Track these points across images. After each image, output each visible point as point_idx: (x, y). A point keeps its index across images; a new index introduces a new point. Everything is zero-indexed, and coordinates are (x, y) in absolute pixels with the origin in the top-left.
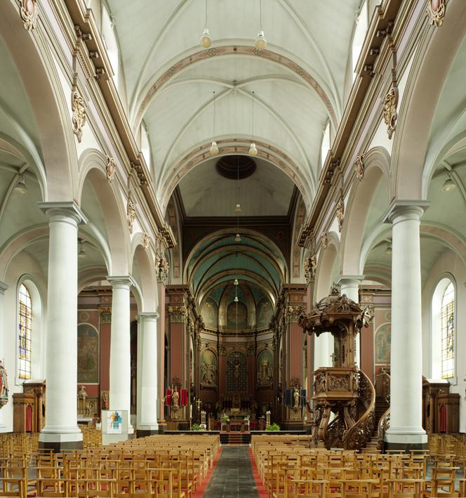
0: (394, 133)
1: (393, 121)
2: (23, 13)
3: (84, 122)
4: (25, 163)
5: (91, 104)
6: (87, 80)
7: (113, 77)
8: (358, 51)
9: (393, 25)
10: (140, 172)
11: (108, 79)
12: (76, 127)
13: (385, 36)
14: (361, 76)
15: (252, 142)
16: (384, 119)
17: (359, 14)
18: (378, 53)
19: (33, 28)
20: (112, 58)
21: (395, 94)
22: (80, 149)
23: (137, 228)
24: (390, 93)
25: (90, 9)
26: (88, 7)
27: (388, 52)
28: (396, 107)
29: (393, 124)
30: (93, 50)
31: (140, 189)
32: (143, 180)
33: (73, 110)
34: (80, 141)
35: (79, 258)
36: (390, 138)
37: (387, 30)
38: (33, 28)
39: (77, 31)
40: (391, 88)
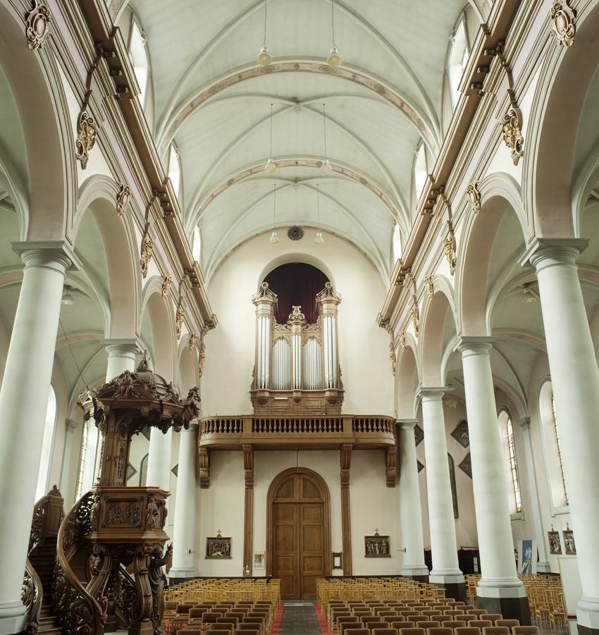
0: (521, 159)
1: (518, 145)
2: (29, 33)
3: (93, 144)
4: (4, 192)
5: (106, 125)
6: (105, 99)
7: (139, 96)
8: (458, 74)
9: (504, 44)
10: (165, 202)
11: (132, 98)
12: (81, 151)
13: (495, 55)
14: (466, 95)
15: (325, 158)
16: (504, 142)
17: (454, 34)
18: (488, 72)
19: (40, 47)
20: (140, 76)
21: (518, 114)
22: (82, 175)
23: (153, 270)
24: (509, 113)
25: (118, 28)
26: (115, 25)
27: (500, 71)
28: (520, 130)
29: (518, 148)
30: (116, 69)
31: (162, 221)
32: (168, 211)
33: (79, 133)
34: (83, 167)
35: (62, 305)
36: (516, 163)
37: (497, 49)
38: (40, 47)
39: (98, 50)
40: (511, 108)
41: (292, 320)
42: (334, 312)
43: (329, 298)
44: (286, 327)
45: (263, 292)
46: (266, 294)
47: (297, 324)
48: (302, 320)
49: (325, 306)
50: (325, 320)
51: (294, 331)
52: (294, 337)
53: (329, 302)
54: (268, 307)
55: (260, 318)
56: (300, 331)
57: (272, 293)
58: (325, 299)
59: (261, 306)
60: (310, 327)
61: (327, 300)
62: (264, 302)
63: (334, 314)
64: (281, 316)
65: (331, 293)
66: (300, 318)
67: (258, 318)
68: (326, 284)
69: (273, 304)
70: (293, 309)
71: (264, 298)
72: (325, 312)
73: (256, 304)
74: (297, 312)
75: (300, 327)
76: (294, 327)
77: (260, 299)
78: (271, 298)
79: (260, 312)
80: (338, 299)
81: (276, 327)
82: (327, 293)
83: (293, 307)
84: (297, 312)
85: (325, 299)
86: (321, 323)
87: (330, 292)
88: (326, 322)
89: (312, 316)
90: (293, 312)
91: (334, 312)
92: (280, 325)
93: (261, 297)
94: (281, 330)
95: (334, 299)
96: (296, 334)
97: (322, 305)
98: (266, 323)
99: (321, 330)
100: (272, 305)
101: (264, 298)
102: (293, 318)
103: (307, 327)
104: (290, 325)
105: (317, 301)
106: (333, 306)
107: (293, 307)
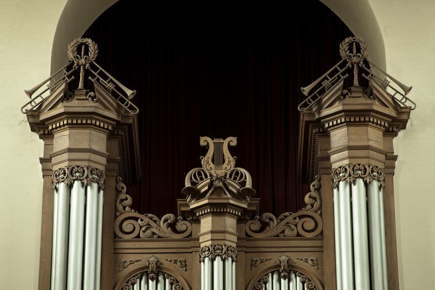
41: (198, 195)
42: (377, 160)
43: (358, 102)
44: (172, 226)
45: (72, 79)
46: (89, 86)
47: (218, 210)
48: (239, 196)
49: (339, 137)
50: (341, 195)
51: (206, 241)
52: (205, 267)
53: (355, 118)
54: (98, 141)
55: (62, 187)
56: (232, 240)
57: (112, 82)
58: (337, 107)
59: (63, 139)
60: (275, 226)
61: (347, 112)
62: (77, 120)
63: (380, 171)
64: (145, 178)
65: (365, 84)
66: (234, 186)
67: (49, 192)
68: (343, 48)
69: (115, 132)
70: (205, 150)
71: (77, 105)
72: (339, 160)
73: (41, 126)
74: (218, 162)
75: (230, 223)
76: (207, 224)
77: (60, 109)
78: (115, 100)
79: (61, 163)
80: (395, 104)
81: (127, 226)
82: (348, 84)
83: (204, 140)
84: (218, 162)
85: (337, 107)
86: (326, 211)
87: (363, 77)
88: (348, 205)
89: (286, 183)
90: (206, 161)
91: (377, 160)
92: (145, 219)
93: (70, 92)
94: (148, 237)
95: (377, 107)
96: (215, 252)
97: (326, 134)
98: (84, 206)
99: (323, 240)
100: (111, 136)
101: (77, 105)
102: (203, 186)
103: (264, 226)
104: (193, 217)
105: (304, 119)
106: (373, 136)
107: (204, 140)
